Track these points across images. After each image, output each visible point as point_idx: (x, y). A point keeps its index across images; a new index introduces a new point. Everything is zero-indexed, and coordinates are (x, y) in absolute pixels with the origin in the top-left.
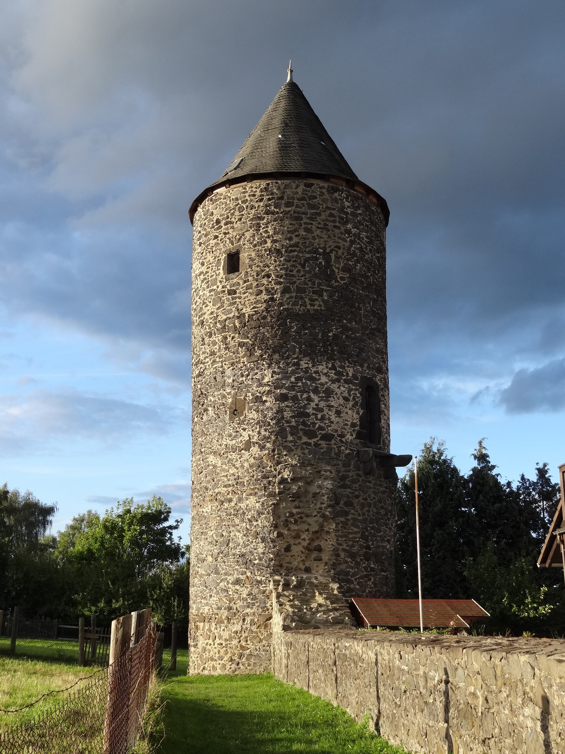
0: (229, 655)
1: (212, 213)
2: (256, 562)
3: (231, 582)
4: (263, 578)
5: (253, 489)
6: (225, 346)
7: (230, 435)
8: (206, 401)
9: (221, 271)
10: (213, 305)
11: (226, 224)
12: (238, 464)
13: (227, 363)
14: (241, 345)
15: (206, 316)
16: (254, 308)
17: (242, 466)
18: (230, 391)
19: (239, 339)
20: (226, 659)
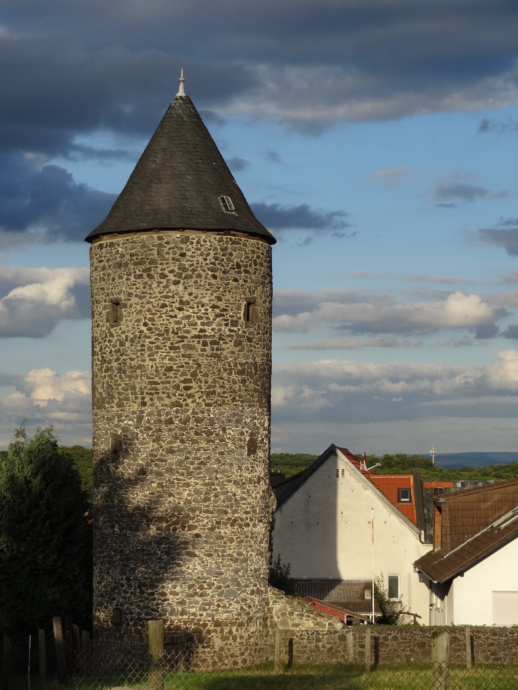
0: (249, 651)
1: (231, 254)
2: (262, 576)
3: (249, 592)
4: (264, 589)
5: (261, 517)
6: (244, 388)
7: (248, 469)
8: (221, 432)
9: (242, 315)
10: (234, 346)
11: (246, 272)
12: (254, 496)
13: (247, 404)
14: (256, 390)
15: (225, 353)
16: (262, 359)
17: (256, 497)
18: (247, 429)
19: (253, 385)
20: (247, 654)
